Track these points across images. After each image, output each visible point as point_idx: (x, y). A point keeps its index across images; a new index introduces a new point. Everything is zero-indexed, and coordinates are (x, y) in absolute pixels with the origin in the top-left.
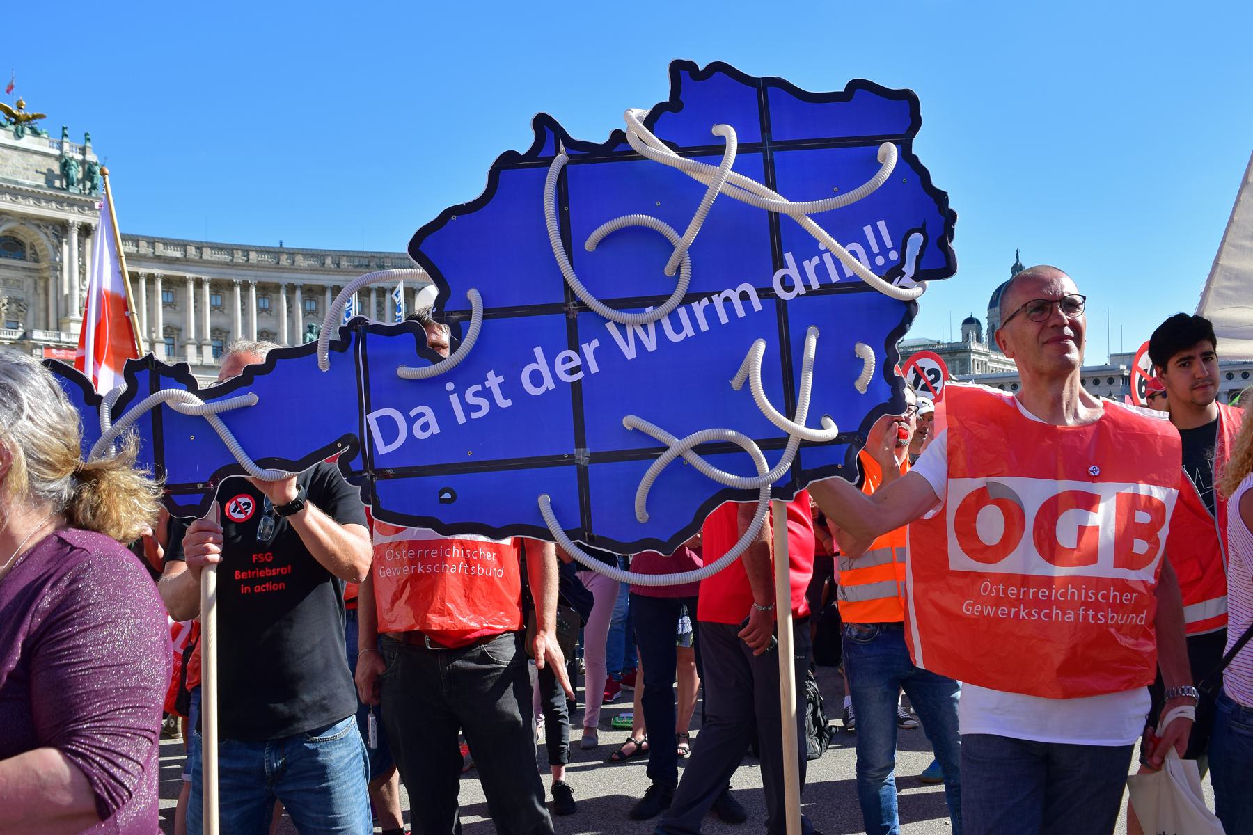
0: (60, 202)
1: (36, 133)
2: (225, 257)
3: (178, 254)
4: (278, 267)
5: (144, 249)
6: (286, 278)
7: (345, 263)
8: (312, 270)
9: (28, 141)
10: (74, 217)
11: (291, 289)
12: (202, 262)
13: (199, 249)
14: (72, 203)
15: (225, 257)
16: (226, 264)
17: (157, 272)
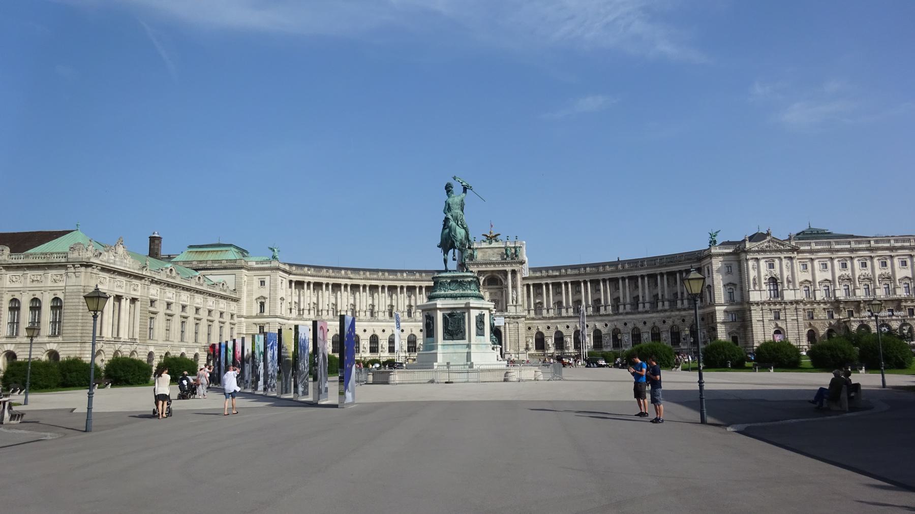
0: (503, 264)
1: (496, 241)
2: (576, 272)
3: (557, 274)
4: (598, 273)
5: (544, 273)
6: (601, 277)
7: (627, 266)
8: (612, 272)
9: (494, 244)
10: (509, 268)
11: (604, 281)
12: (567, 275)
13: (566, 270)
14: (507, 263)
15: (576, 272)
16: (576, 275)
17: (549, 281)
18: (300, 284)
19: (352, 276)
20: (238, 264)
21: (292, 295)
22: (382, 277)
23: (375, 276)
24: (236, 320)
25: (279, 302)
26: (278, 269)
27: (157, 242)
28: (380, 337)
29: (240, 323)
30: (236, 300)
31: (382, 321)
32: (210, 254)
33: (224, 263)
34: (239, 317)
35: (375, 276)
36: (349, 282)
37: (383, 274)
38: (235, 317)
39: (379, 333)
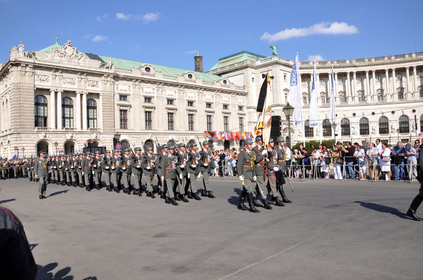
18: (306, 77)
19: (356, 64)
20: (245, 64)
21: (302, 87)
22: (388, 61)
23: (381, 61)
24: (245, 110)
25: (283, 93)
26: (277, 63)
27: (198, 60)
28: (390, 119)
29: (250, 113)
30: (245, 94)
31: (390, 103)
32: (231, 61)
33: (237, 66)
34: (249, 108)
35: (381, 61)
36: (354, 70)
37: (390, 58)
38: (244, 108)
39: (389, 115)
